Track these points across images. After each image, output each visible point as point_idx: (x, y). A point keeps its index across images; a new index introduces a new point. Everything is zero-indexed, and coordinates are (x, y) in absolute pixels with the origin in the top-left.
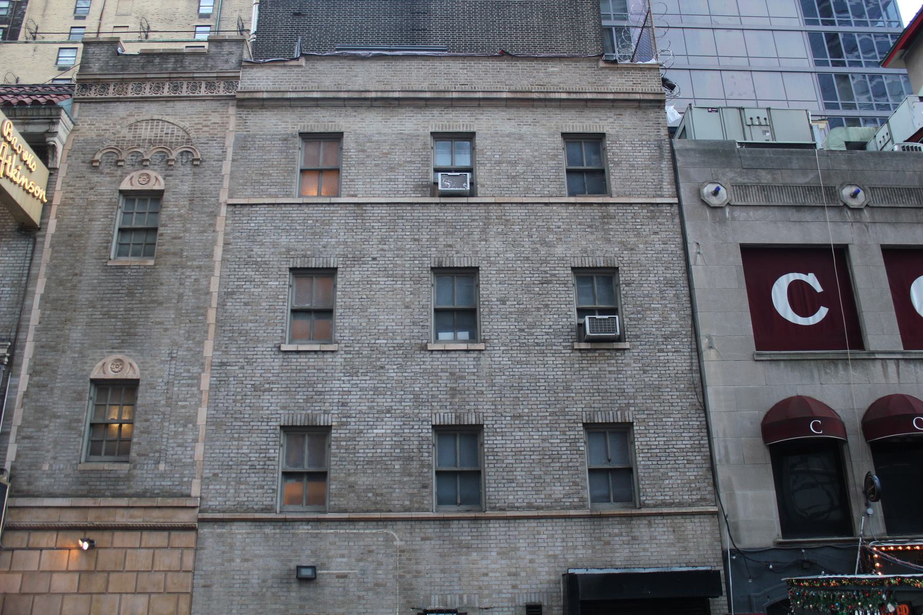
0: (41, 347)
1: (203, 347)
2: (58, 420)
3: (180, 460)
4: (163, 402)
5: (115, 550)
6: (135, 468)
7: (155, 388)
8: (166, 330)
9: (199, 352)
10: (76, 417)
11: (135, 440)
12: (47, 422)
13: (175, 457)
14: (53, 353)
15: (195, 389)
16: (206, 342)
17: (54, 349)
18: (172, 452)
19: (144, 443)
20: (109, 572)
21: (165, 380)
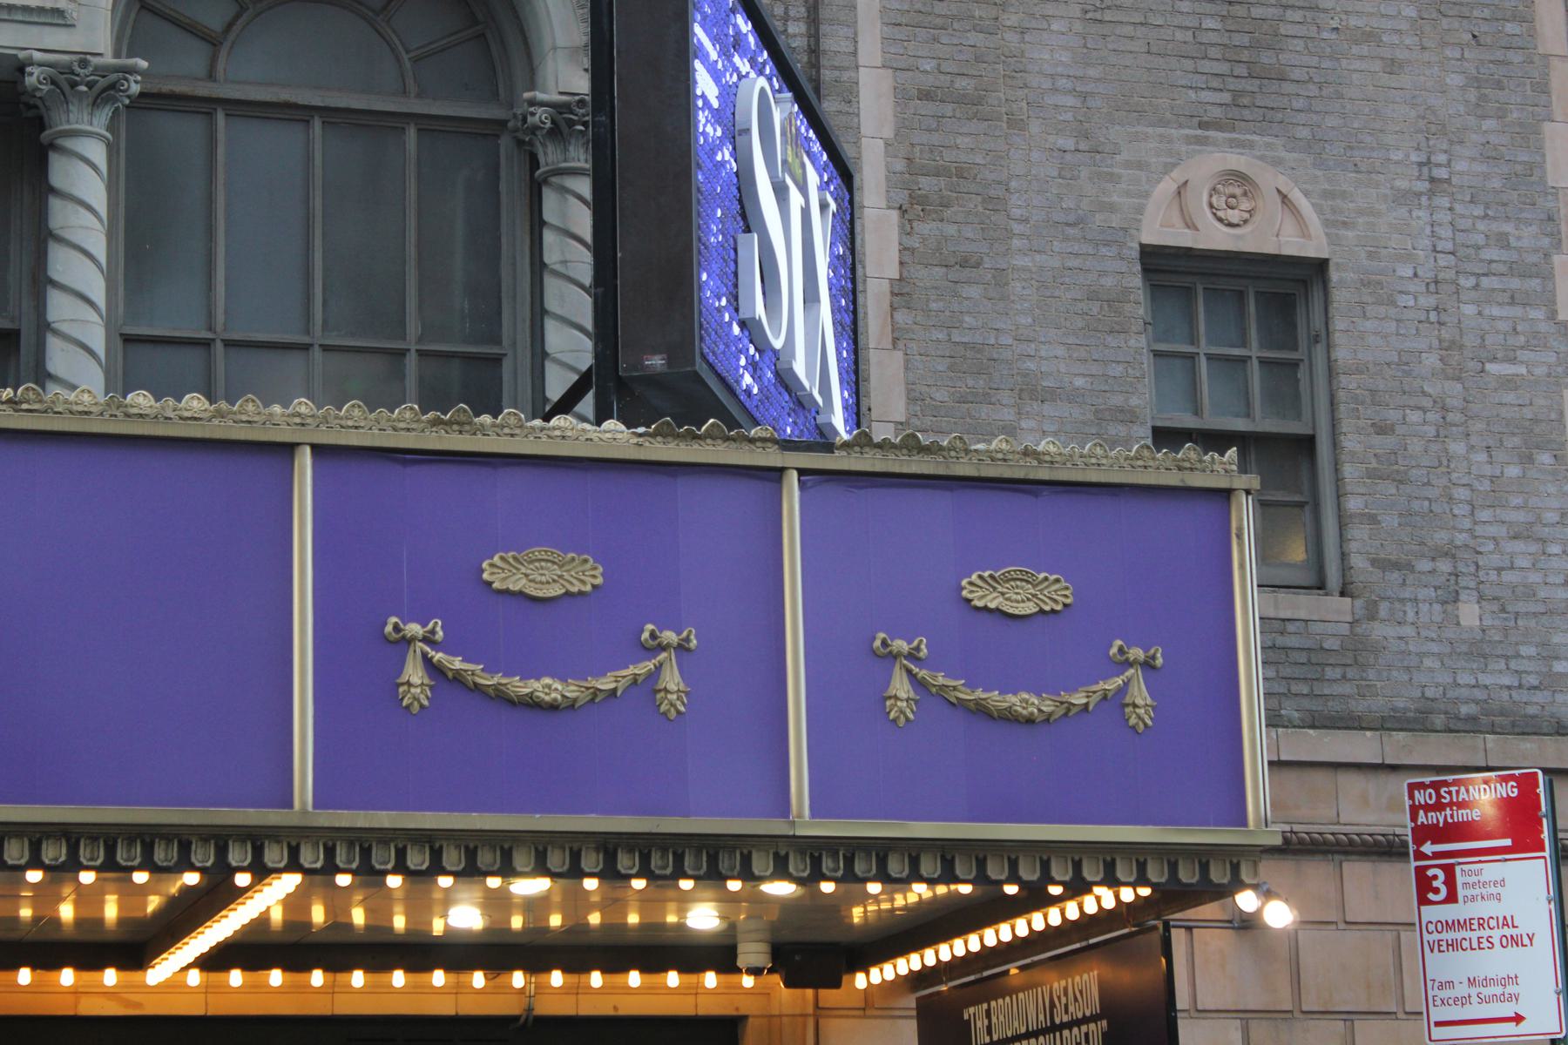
0: (917, 97)
1: (1540, 149)
2: (1047, 409)
3: (1530, 593)
4: (1431, 360)
5: (1353, 936)
6: (1372, 617)
7: (1393, 303)
8: (1393, 66)
9: (1531, 167)
10: (1117, 400)
11: (1353, 504)
12: (1008, 415)
13: (1508, 577)
14: (974, 126)
15: (1537, 314)
16: (1547, 127)
17: (972, 104)
18: (1495, 560)
19: (1390, 521)
20: (1349, 1016)
21: (1426, 273)
